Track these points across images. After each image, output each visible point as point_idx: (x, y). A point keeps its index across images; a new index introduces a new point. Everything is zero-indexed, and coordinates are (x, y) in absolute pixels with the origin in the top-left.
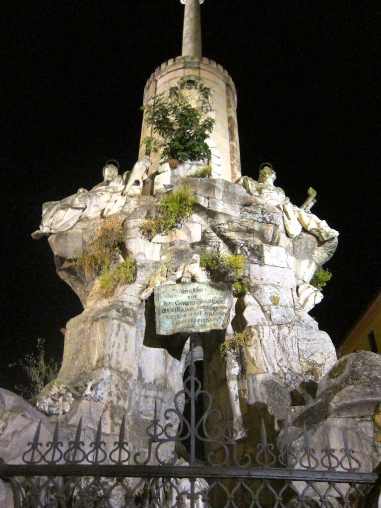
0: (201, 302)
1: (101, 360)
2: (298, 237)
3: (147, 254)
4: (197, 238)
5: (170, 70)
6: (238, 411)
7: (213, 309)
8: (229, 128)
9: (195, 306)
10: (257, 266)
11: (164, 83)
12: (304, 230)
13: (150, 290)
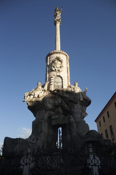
0: (61, 117)
3: (49, 107)
4: (60, 102)
9: (60, 118)
10: (73, 109)
12: (84, 99)
13: (50, 115)
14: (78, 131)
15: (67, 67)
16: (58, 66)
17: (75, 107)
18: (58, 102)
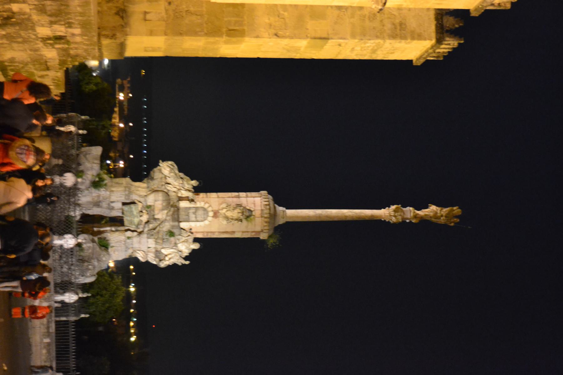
1: (113, 191)
2: (162, 253)
4: (156, 217)
6: (102, 229)
7: (131, 222)
12: (166, 256)
15: (234, 232)
16: (229, 214)
17: (150, 240)
18: (158, 214)
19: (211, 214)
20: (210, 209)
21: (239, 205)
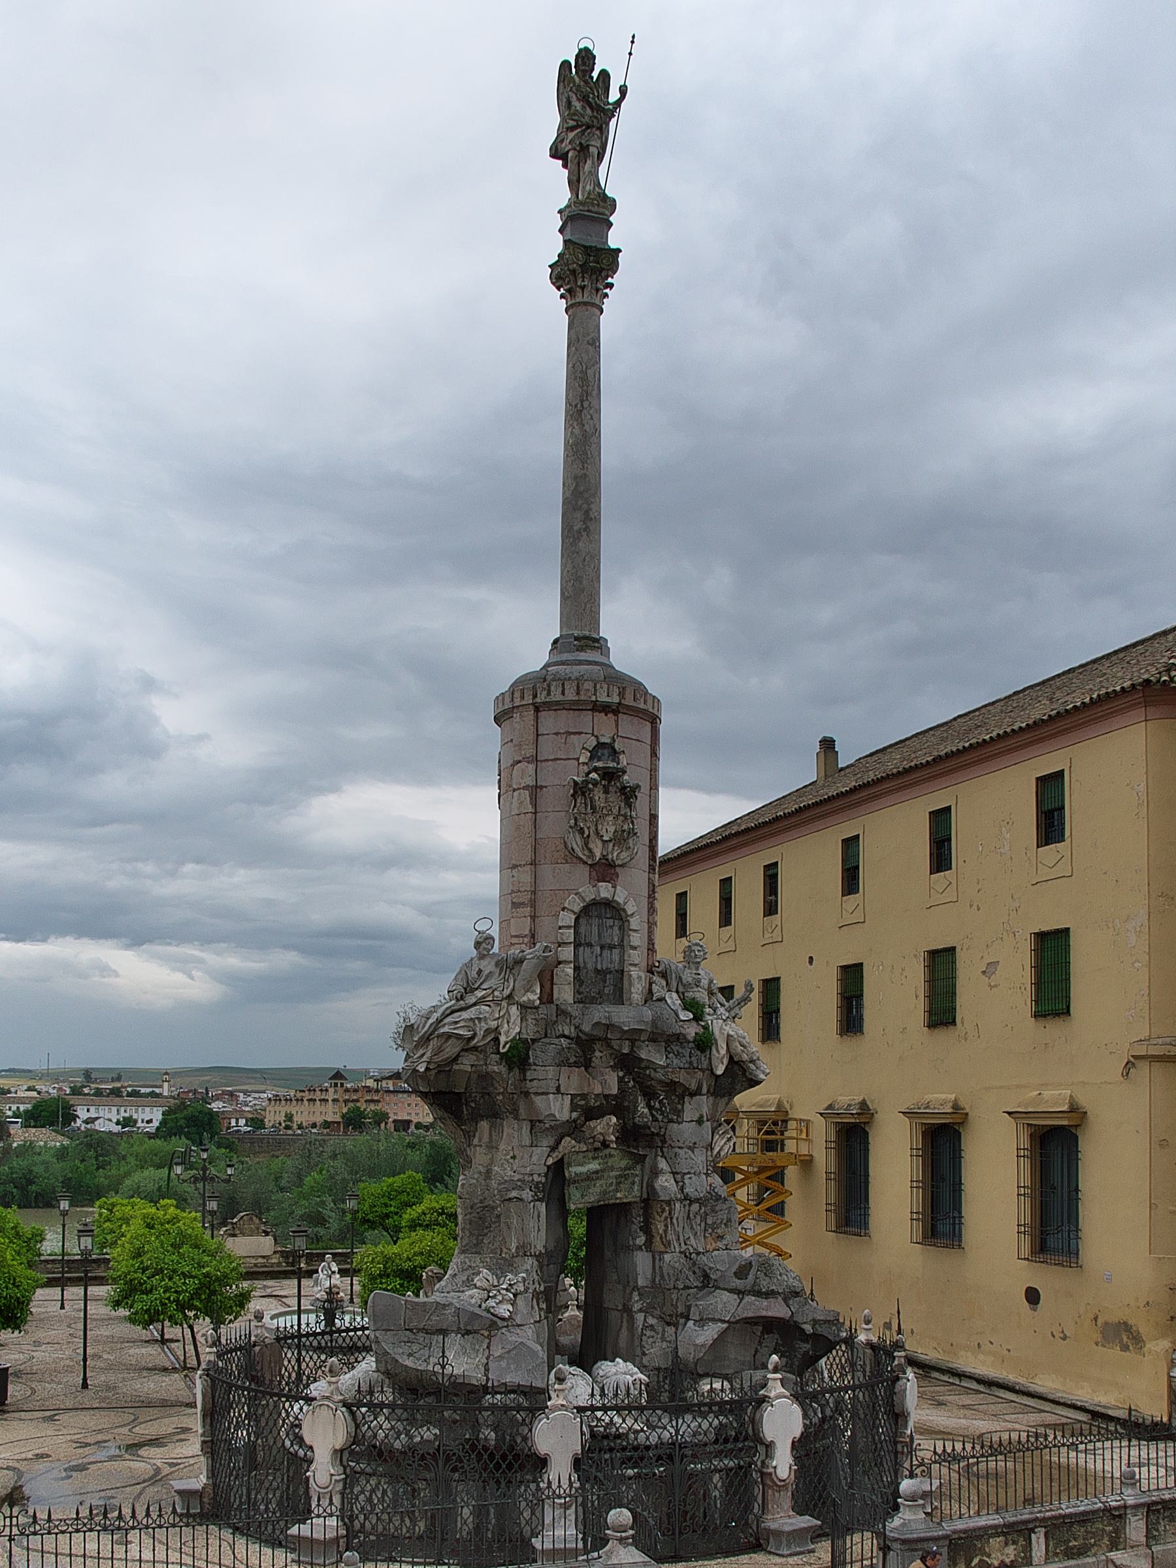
4: (615, 1091)
5: (567, 706)
8: (651, 841)
9: (606, 1175)
11: (556, 734)
13: (556, 1155)
14: (693, 1241)
16: (608, 829)
18: (604, 1083)
19: (605, 891)
20: (589, 894)
21: (580, 790)
